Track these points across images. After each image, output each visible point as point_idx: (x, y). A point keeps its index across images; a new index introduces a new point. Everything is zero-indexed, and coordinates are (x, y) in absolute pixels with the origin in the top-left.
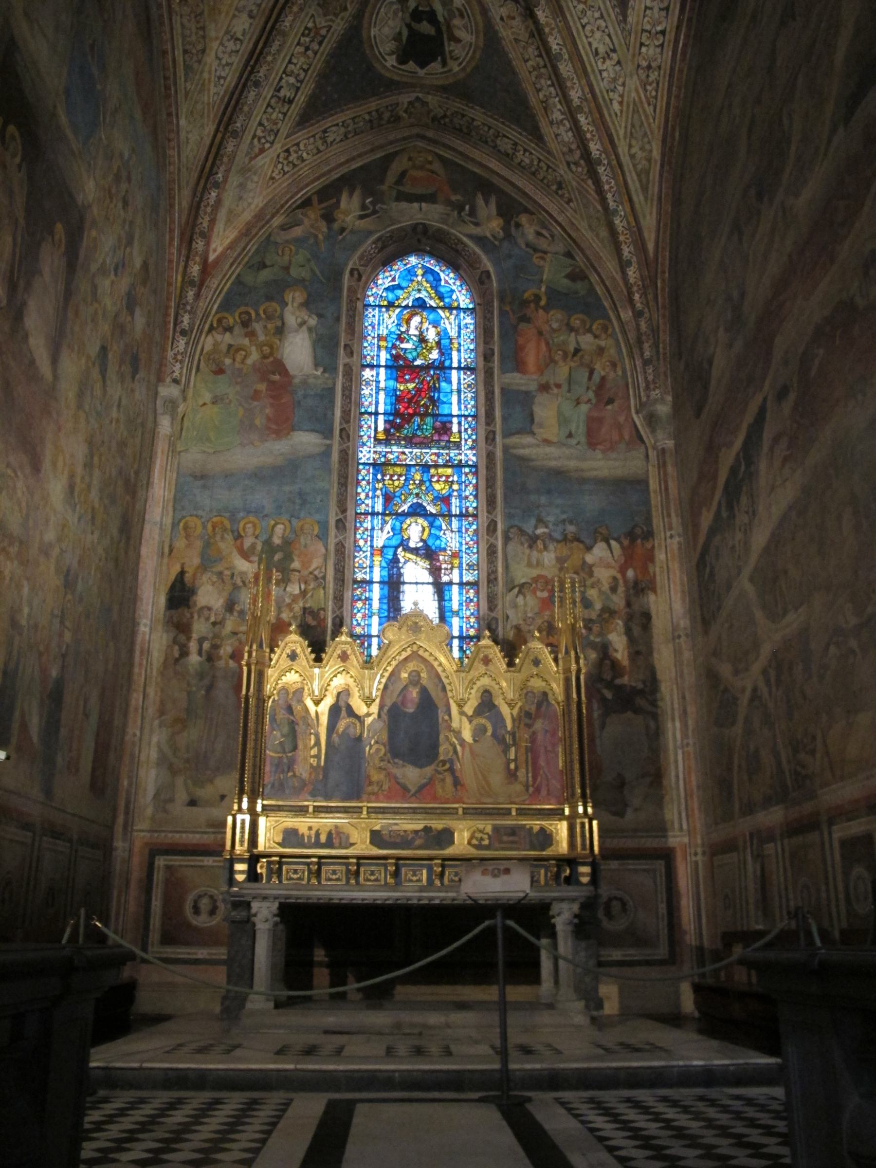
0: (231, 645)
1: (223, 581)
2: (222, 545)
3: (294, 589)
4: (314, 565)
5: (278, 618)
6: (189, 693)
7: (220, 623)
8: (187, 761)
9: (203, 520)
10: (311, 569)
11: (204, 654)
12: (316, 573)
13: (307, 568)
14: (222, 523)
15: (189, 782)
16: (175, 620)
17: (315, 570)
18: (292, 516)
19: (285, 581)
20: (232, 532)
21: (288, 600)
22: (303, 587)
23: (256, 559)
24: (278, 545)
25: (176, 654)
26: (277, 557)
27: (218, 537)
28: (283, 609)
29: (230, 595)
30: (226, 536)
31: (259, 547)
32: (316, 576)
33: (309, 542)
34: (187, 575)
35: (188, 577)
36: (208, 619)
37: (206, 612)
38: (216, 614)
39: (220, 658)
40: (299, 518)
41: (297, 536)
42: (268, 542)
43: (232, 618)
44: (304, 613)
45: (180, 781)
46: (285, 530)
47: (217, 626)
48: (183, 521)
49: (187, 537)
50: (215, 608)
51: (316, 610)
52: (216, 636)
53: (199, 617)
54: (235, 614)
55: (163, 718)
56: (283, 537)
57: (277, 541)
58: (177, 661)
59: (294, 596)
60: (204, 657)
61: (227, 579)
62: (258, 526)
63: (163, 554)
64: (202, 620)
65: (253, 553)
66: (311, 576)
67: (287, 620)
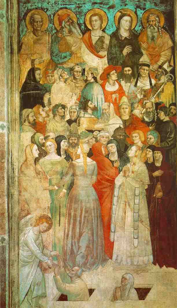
0: (88, 143)
1: (75, 78)
2: (70, 39)
3: (145, 83)
4: (162, 60)
5: (132, 115)
6: (51, 192)
7: (75, 121)
8: (56, 257)
9: (49, 13)
10: (160, 63)
11: (62, 153)
12: (165, 66)
13: (156, 62)
14: (69, 15)
15: (59, 277)
16: (31, 119)
17: (163, 63)
18: (138, 7)
19: (136, 75)
20: (80, 25)
21: (139, 97)
22: (153, 82)
23: (104, 53)
24: (126, 38)
25: (36, 154)
26: (126, 50)
27: (66, 31)
28: (136, 105)
29: (82, 92)
30: (73, 29)
31: (107, 41)
32: (165, 71)
33: (155, 34)
34: (38, 72)
35: (38, 75)
36: (63, 117)
37: (61, 110)
38: (70, 112)
39: (78, 157)
40: (144, 9)
41: (143, 28)
42: (115, 35)
43: (86, 115)
44: (156, 109)
45: (50, 276)
46: (131, 22)
47: (73, 124)
48: (29, 14)
49: (35, 32)
50: (69, 106)
51: (168, 106)
52: (72, 134)
53: (55, 115)
54: (90, 111)
55: (29, 216)
56: (130, 30)
57: (124, 34)
58: (36, 160)
59: (145, 91)
60: (63, 157)
61: (78, 76)
62: (104, 18)
63: (12, 49)
64: (58, 118)
65: (102, 48)
66: (160, 70)
67: (140, 116)
